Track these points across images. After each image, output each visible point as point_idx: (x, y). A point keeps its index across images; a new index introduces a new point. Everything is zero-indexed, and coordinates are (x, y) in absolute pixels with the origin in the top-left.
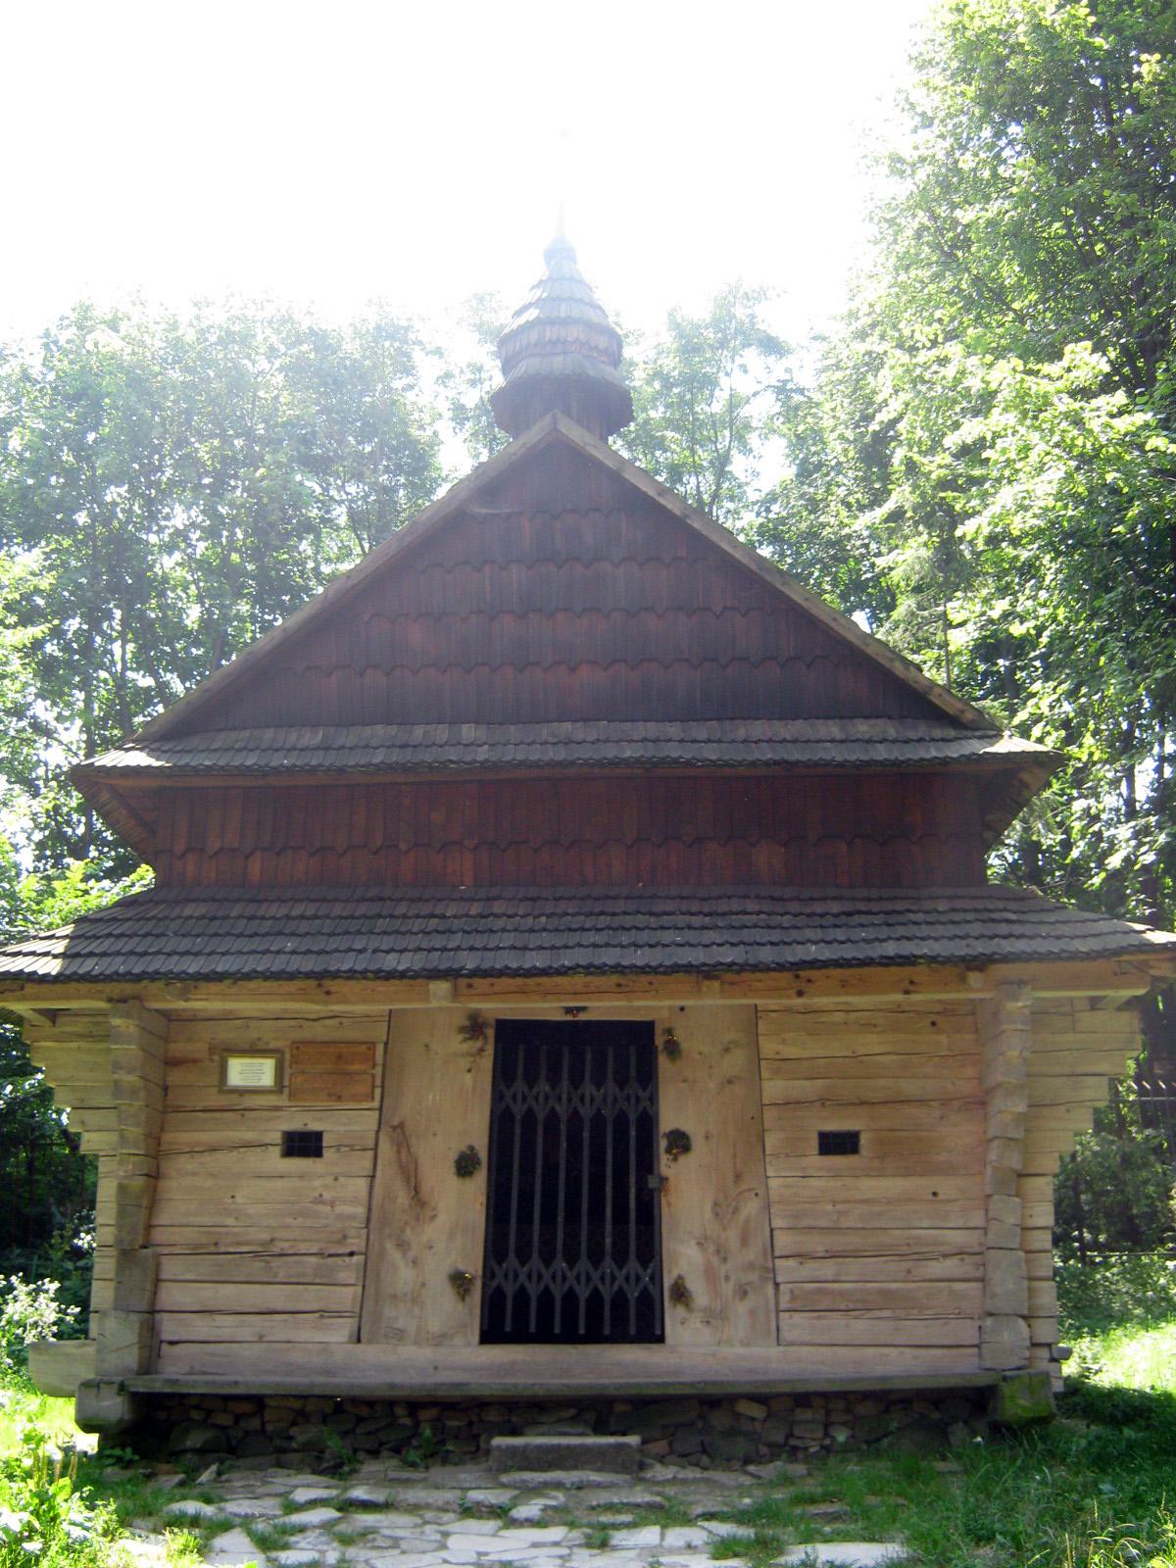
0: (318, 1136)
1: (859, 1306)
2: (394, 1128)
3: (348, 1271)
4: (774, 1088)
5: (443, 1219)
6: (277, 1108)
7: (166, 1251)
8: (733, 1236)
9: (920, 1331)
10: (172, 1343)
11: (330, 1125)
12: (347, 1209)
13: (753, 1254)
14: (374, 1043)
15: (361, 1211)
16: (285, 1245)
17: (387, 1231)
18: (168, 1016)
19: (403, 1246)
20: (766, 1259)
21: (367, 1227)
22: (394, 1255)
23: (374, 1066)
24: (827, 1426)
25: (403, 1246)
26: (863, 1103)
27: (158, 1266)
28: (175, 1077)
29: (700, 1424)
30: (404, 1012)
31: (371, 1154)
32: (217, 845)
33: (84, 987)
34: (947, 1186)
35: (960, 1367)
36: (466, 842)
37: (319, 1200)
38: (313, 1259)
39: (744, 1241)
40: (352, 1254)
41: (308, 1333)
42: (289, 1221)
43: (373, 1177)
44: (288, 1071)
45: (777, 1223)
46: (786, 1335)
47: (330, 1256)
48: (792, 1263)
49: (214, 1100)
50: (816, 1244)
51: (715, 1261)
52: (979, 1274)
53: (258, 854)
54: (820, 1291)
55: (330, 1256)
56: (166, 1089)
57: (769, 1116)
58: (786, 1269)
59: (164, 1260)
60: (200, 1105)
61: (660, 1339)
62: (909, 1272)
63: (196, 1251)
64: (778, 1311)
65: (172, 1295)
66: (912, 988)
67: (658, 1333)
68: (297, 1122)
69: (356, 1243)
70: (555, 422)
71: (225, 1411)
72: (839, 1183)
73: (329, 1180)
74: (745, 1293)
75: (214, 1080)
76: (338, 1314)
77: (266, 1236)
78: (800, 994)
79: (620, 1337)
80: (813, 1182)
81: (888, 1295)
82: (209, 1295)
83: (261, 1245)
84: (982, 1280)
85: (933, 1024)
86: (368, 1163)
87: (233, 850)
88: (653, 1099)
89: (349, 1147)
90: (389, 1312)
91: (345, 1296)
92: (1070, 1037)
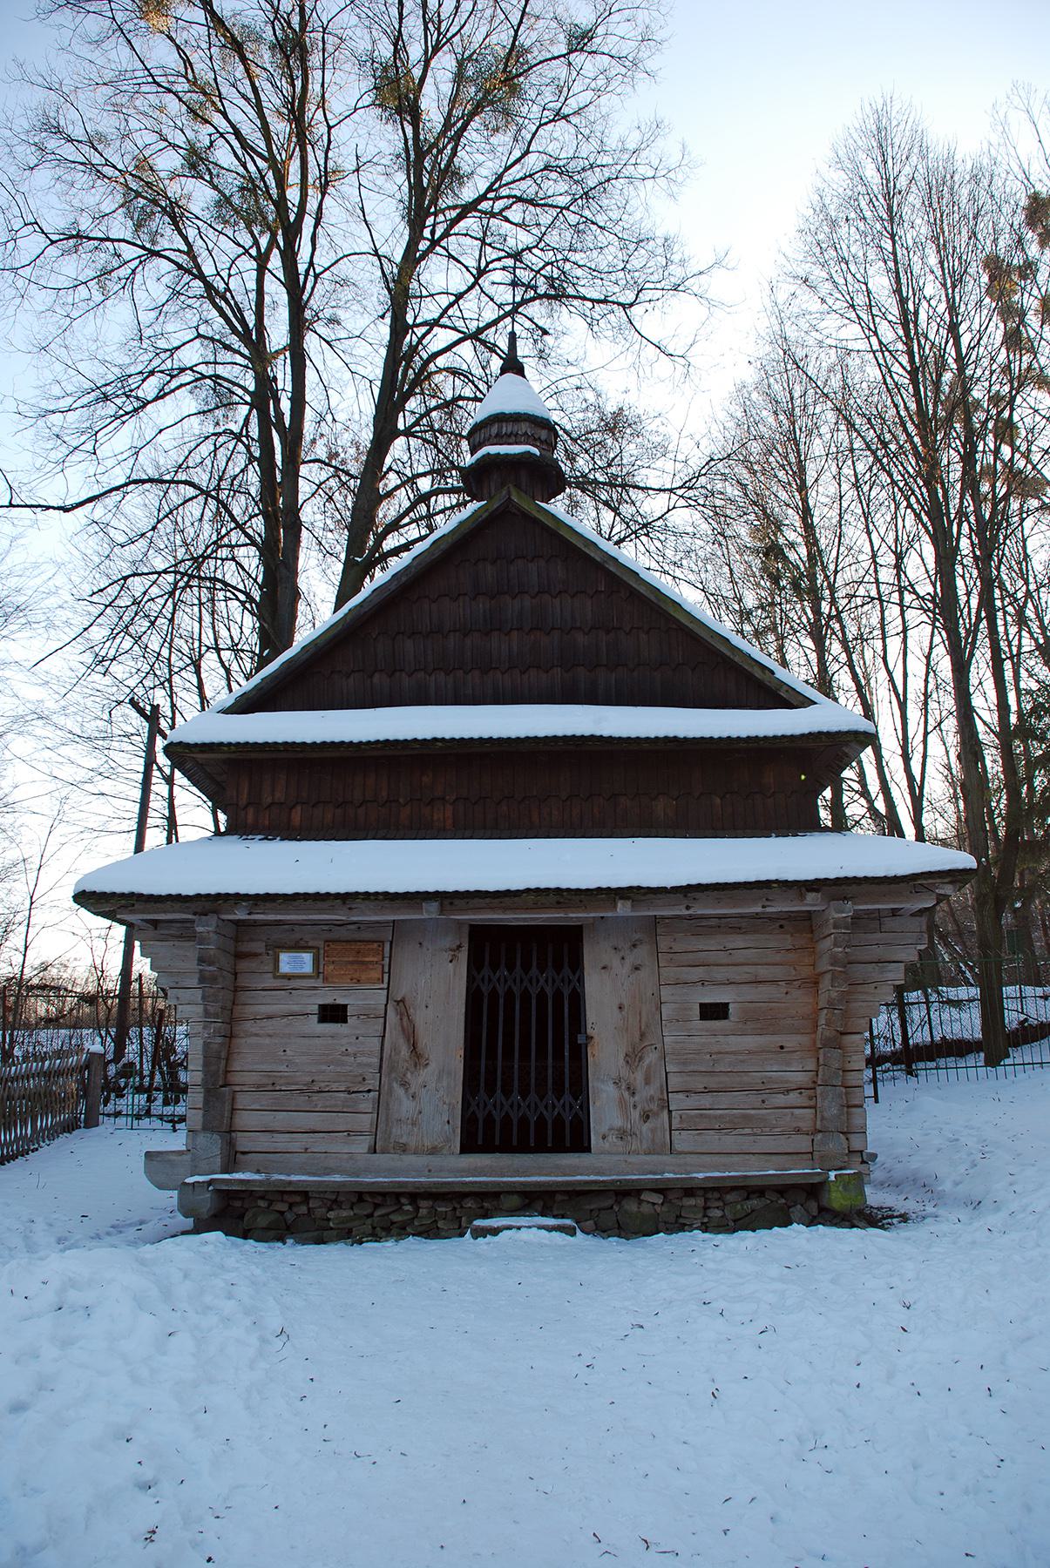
0: (345, 1007)
1: (728, 1126)
2: (398, 1002)
3: (366, 1103)
5: (433, 1066)
6: (315, 988)
7: (237, 1088)
8: (639, 1077)
9: (767, 1144)
10: (244, 1153)
11: (351, 999)
12: (364, 1060)
13: (653, 1090)
14: (383, 942)
15: (376, 1060)
16: (323, 1085)
17: (393, 1075)
19: (405, 1084)
20: (662, 1093)
21: (380, 1072)
22: (400, 1091)
24: (706, 1208)
25: (405, 1084)
26: (731, 983)
27: (233, 1099)
28: (243, 965)
29: (616, 1208)
31: (382, 1020)
32: (269, 800)
33: (177, 906)
34: (791, 1041)
35: (800, 1170)
36: (447, 797)
38: (342, 1095)
39: (647, 1082)
40: (369, 1091)
41: (337, 1146)
42: (324, 1067)
43: (384, 1036)
44: (322, 962)
46: (678, 1146)
47: (354, 1092)
48: (681, 1096)
49: (269, 982)
51: (626, 1094)
52: (812, 1103)
53: (299, 808)
54: (701, 1115)
55: (354, 1092)
56: (236, 974)
57: (666, 993)
58: (677, 1101)
59: (239, 1097)
61: (588, 1149)
62: (763, 1102)
63: (259, 1088)
64: (671, 1130)
65: (245, 1120)
66: (768, 903)
67: (586, 1145)
68: (329, 998)
69: (373, 1083)
70: (509, 493)
71: (282, 1201)
72: (713, 1040)
73: (353, 1039)
74: (648, 1117)
75: (270, 968)
76: (361, 1133)
78: (688, 908)
79: (559, 1148)
80: (696, 1039)
81: (745, 1117)
82: (270, 1120)
83: (305, 1085)
84: (814, 1107)
85: (781, 927)
86: (380, 1028)
87: (282, 804)
88: (581, 980)
89: (366, 1015)
90: (396, 1131)
91: (365, 1121)
92: (878, 935)
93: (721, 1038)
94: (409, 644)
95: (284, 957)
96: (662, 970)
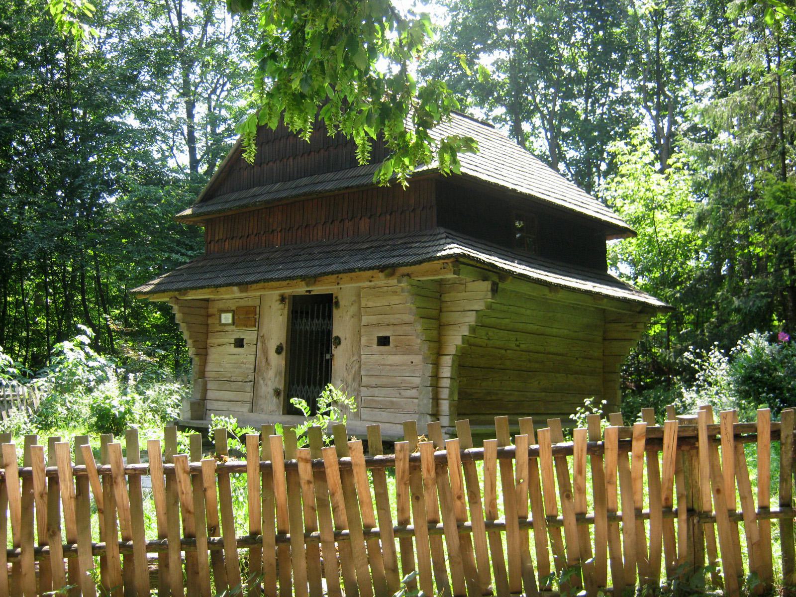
0: (242, 340)
3: (249, 387)
4: (365, 320)
6: (233, 331)
8: (350, 377)
12: (248, 366)
14: (256, 307)
15: (252, 366)
18: (207, 300)
19: (264, 379)
23: (256, 315)
30: (264, 295)
37: (242, 363)
38: (240, 383)
44: (236, 317)
45: (363, 373)
48: (365, 389)
49: (219, 328)
50: (373, 381)
57: (363, 330)
60: (216, 330)
66: (373, 279)
68: (238, 335)
72: (382, 357)
75: (217, 322)
76: (246, 402)
77: (230, 375)
80: (375, 357)
81: (392, 402)
86: (255, 350)
88: (332, 324)
91: (248, 396)
92: (464, 294)
93: (385, 356)
94: (267, 147)
95: (223, 315)
96: (363, 317)
